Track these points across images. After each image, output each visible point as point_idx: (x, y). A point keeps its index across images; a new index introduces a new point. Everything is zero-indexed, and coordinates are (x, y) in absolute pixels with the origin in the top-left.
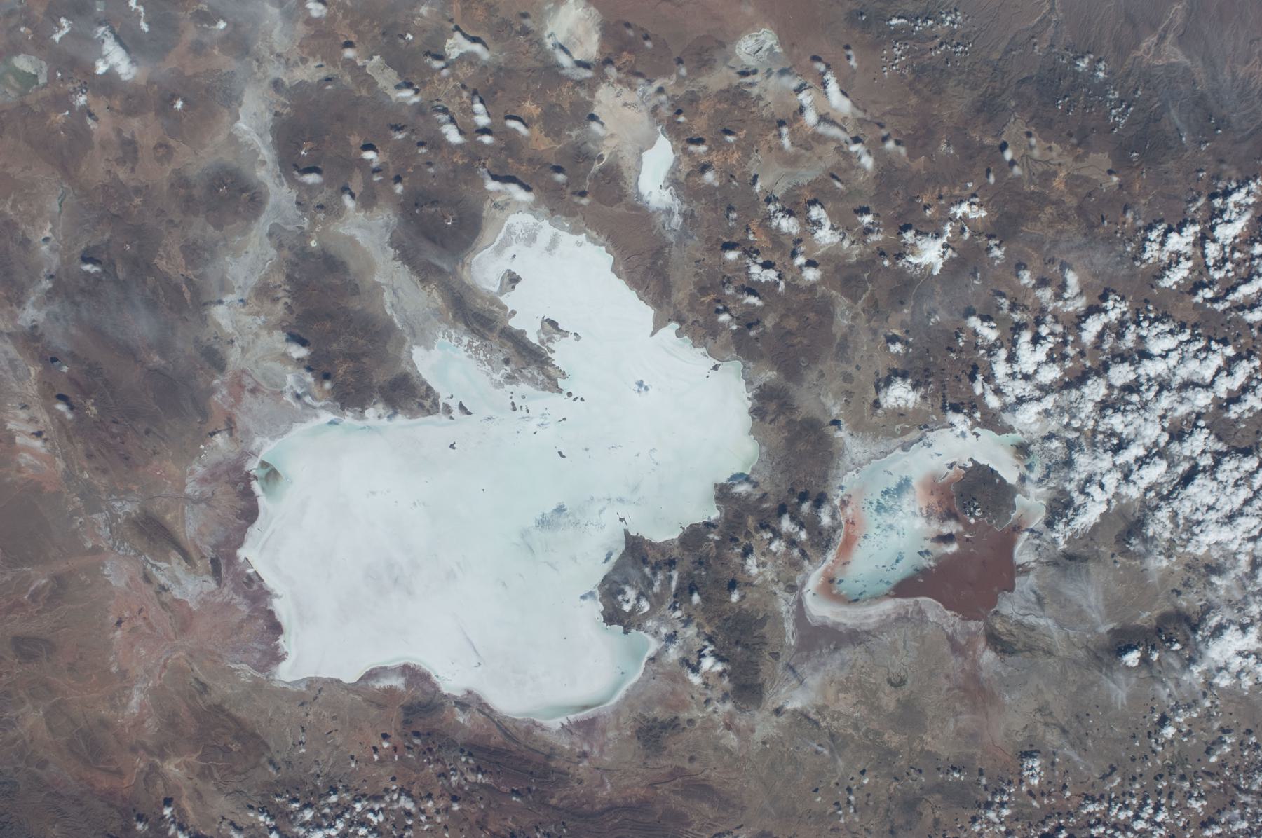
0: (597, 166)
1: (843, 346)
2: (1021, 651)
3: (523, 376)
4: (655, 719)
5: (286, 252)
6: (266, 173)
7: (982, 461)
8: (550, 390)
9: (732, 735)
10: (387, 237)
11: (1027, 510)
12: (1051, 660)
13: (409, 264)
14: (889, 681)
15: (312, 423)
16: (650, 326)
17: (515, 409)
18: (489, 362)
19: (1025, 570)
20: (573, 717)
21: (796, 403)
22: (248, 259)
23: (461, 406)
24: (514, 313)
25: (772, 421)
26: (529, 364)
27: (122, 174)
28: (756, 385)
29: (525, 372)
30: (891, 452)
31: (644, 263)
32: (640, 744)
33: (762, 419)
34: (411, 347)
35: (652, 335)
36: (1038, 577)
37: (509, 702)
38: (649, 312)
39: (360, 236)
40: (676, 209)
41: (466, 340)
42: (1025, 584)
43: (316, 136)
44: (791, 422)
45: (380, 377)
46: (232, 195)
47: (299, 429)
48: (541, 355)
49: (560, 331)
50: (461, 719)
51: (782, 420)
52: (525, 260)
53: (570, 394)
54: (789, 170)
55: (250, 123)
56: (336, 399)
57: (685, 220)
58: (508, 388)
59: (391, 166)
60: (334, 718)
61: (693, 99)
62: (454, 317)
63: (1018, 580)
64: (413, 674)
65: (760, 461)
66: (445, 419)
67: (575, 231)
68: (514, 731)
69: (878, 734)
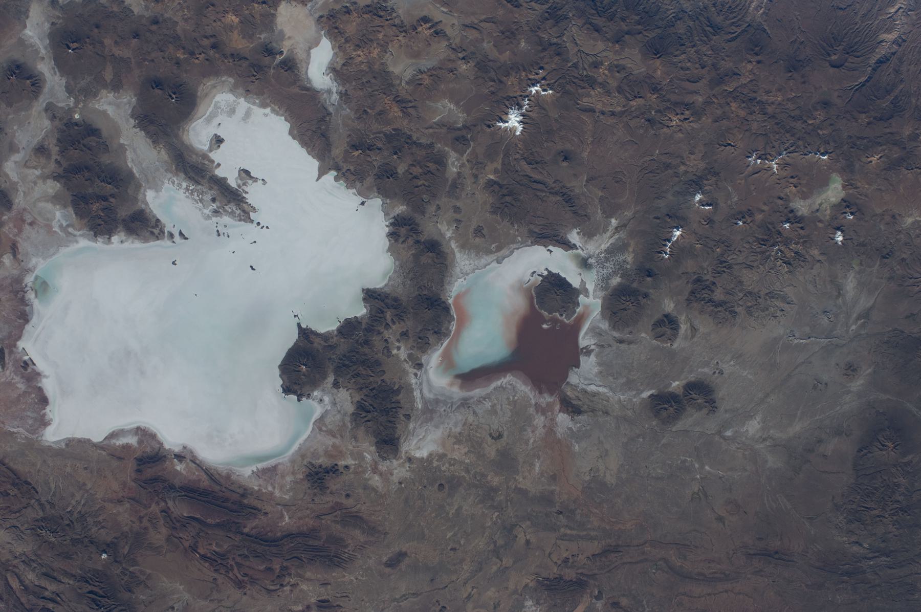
0: (279, 58)
2: (586, 412)
3: (225, 211)
4: (320, 466)
5: (57, 122)
7: (555, 271)
8: (244, 220)
9: (377, 478)
10: (130, 112)
11: (587, 307)
12: (608, 418)
13: (144, 130)
14: (491, 435)
15: (74, 247)
16: (316, 173)
17: (219, 235)
18: (201, 200)
19: (588, 352)
20: (260, 466)
21: (420, 229)
23: (181, 234)
24: (219, 165)
25: (404, 241)
26: (229, 202)
28: (392, 216)
29: (227, 208)
30: (489, 264)
32: (309, 485)
33: (396, 241)
34: (145, 190)
35: (317, 180)
36: (597, 356)
37: (213, 455)
38: (314, 164)
39: (110, 110)
40: (334, 90)
41: (184, 185)
42: (589, 364)
44: (418, 242)
45: (123, 212)
47: (64, 251)
48: (240, 195)
49: (251, 177)
50: (178, 468)
51: (410, 241)
52: (227, 127)
53: (258, 224)
54: (414, 61)
56: (91, 229)
57: (341, 97)
58: (214, 219)
59: (133, 60)
60: (86, 468)
62: (176, 168)
63: (583, 359)
64: (143, 433)
65: (395, 272)
66: (169, 243)
67: (263, 105)
68: (217, 477)
69: (483, 476)
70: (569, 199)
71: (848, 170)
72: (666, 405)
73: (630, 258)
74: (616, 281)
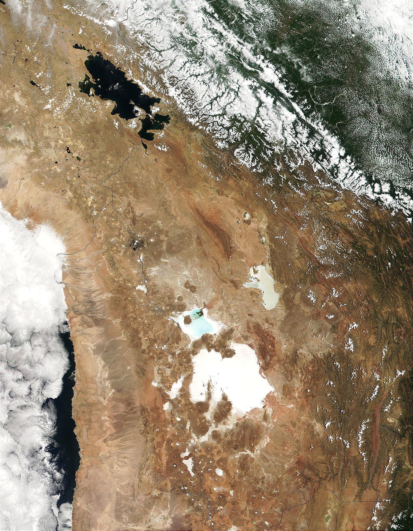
1: (182, 349)
6: (210, 432)
22: (222, 428)
27: (222, 451)
31: (188, 379)
38: (194, 375)
43: (202, 430)
45: (225, 402)
46: (216, 435)
55: (205, 438)
61: (166, 387)
64: (260, 373)
70: (171, 330)
71: (135, 288)
72: (193, 289)
73: (173, 313)
74: (178, 312)
